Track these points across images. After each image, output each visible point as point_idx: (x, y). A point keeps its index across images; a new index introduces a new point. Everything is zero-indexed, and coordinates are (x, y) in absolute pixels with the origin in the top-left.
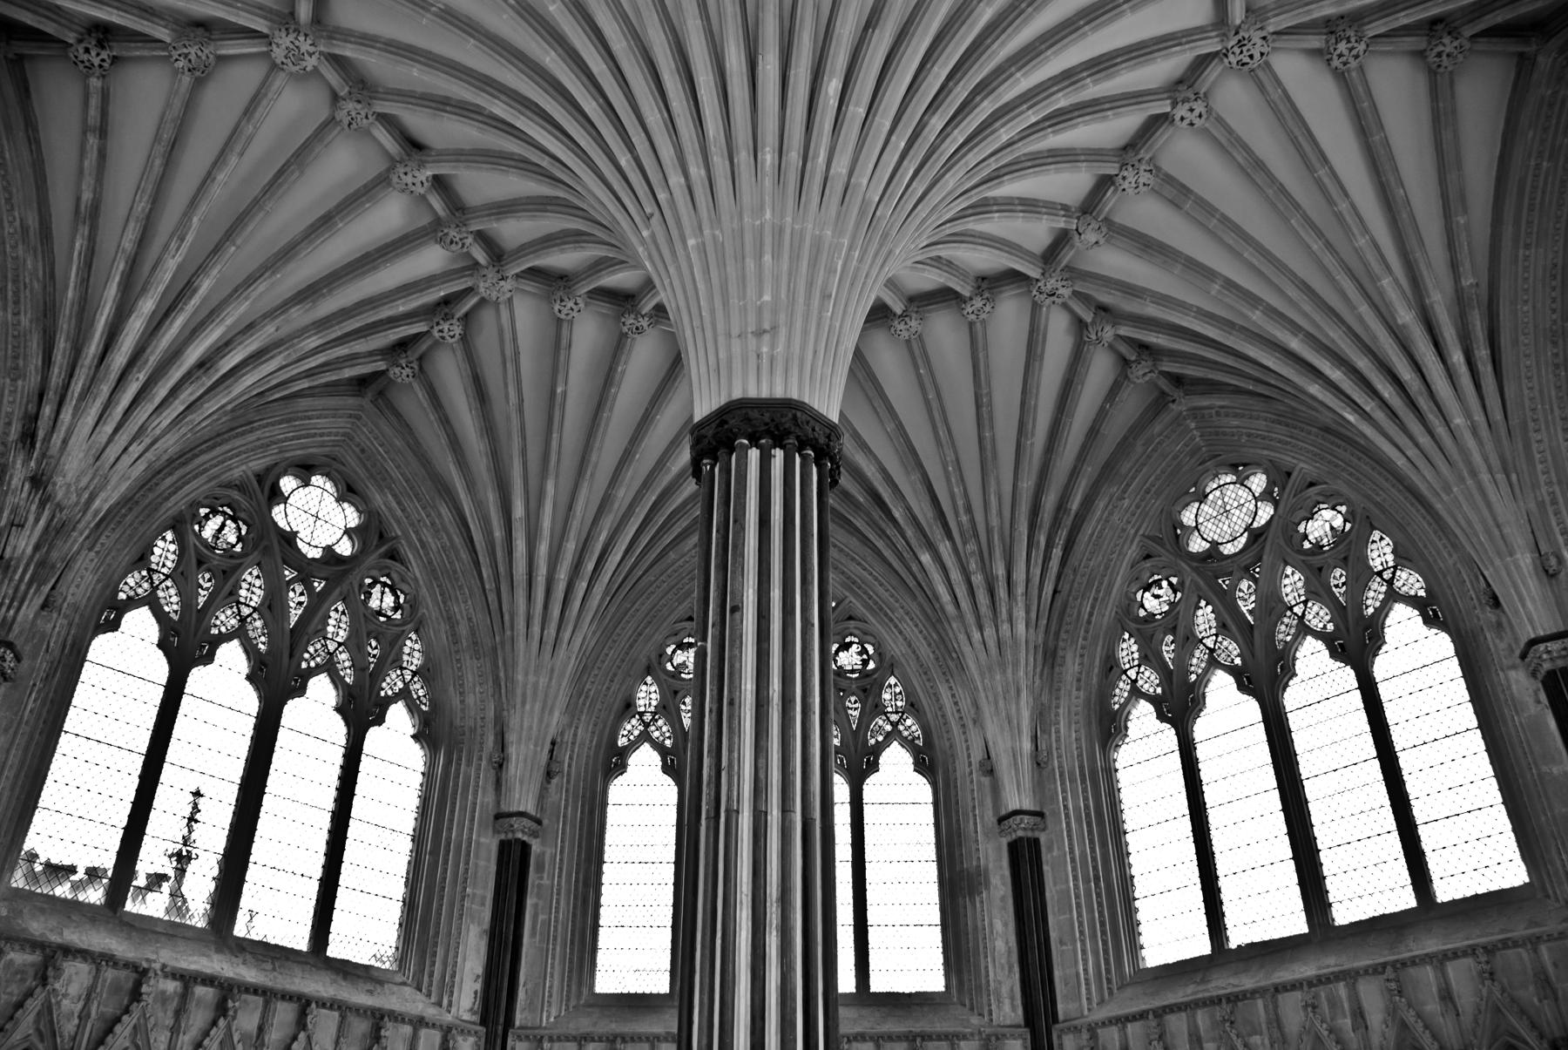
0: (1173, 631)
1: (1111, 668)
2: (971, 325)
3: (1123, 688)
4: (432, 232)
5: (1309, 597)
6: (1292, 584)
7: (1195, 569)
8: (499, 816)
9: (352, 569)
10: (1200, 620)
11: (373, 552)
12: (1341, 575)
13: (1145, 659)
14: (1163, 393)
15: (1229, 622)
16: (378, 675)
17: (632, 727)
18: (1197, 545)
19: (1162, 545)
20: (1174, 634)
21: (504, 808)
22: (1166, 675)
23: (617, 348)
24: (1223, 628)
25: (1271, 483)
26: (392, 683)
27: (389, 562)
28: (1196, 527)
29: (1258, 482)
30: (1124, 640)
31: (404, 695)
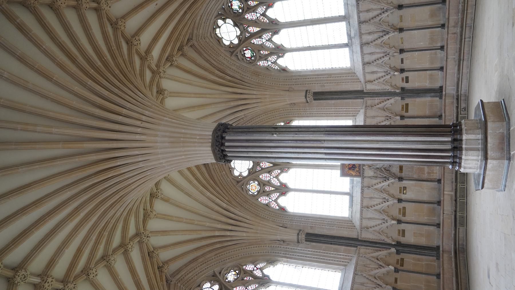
0: (259, 51)
1: (267, 69)
2: (169, 96)
3: (273, 66)
4: (126, 254)
5: (255, 11)
6: (249, 16)
7: (243, 42)
8: (298, 242)
9: (224, 285)
10: (258, 43)
11: (219, 278)
12: (250, 2)
13: (266, 60)
14: (191, 46)
15: (258, 35)
16: (255, 277)
17: (274, 205)
18: (236, 42)
19: (234, 51)
20: (260, 51)
21: (297, 241)
22: (271, 54)
23: (166, 200)
24: (260, 37)
25: (221, 19)
26: (258, 273)
27: (222, 273)
28: (231, 41)
29: (220, 22)
30: (260, 65)
31: (261, 269)
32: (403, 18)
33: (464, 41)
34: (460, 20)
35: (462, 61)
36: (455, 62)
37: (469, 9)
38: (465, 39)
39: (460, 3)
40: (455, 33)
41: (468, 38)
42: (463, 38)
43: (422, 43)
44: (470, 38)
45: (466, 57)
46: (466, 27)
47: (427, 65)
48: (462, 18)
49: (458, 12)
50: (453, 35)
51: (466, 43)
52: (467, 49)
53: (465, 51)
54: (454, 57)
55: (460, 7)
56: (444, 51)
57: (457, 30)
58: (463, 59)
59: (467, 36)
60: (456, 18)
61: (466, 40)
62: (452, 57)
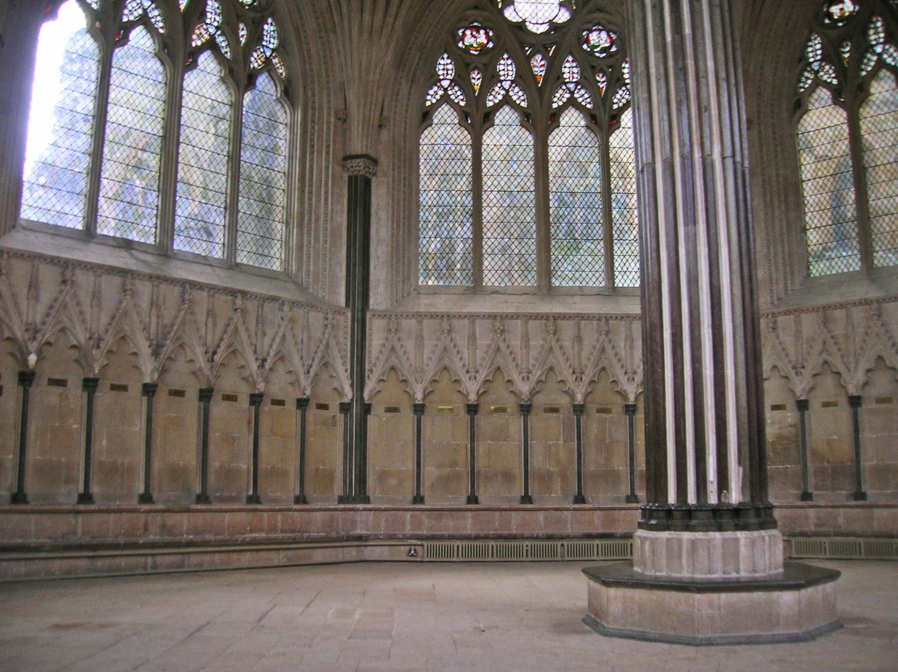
32: (177, 399)
33: (147, 555)
34: (178, 538)
35: (91, 554)
36: (63, 537)
37: (222, 556)
38: (153, 555)
39: (216, 534)
40: (146, 529)
41: (155, 562)
42: (154, 551)
43: (104, 442)
44: (154, 567)
45: (99, 563)
46: (183, 554)
47: (34, 455)
48: (211, 541)
49: (197, 534)
50: (141, 524)
51: (142, 560)
52: (123, 563)
53: (117, 560)
54: (80, 531)
55: (208, 537)
56: (79, 502)
57: (156, 535)
58: (94, 557)
59: (159, 559)
60: (185, 528)
61: (150, 560)
62: (80, 525)
